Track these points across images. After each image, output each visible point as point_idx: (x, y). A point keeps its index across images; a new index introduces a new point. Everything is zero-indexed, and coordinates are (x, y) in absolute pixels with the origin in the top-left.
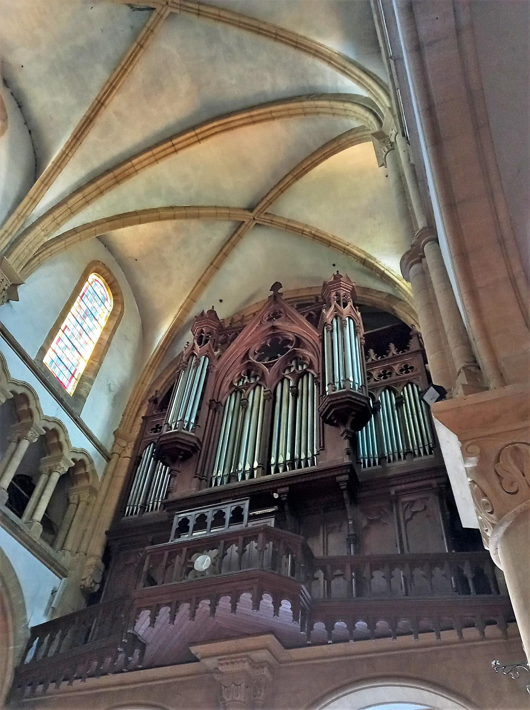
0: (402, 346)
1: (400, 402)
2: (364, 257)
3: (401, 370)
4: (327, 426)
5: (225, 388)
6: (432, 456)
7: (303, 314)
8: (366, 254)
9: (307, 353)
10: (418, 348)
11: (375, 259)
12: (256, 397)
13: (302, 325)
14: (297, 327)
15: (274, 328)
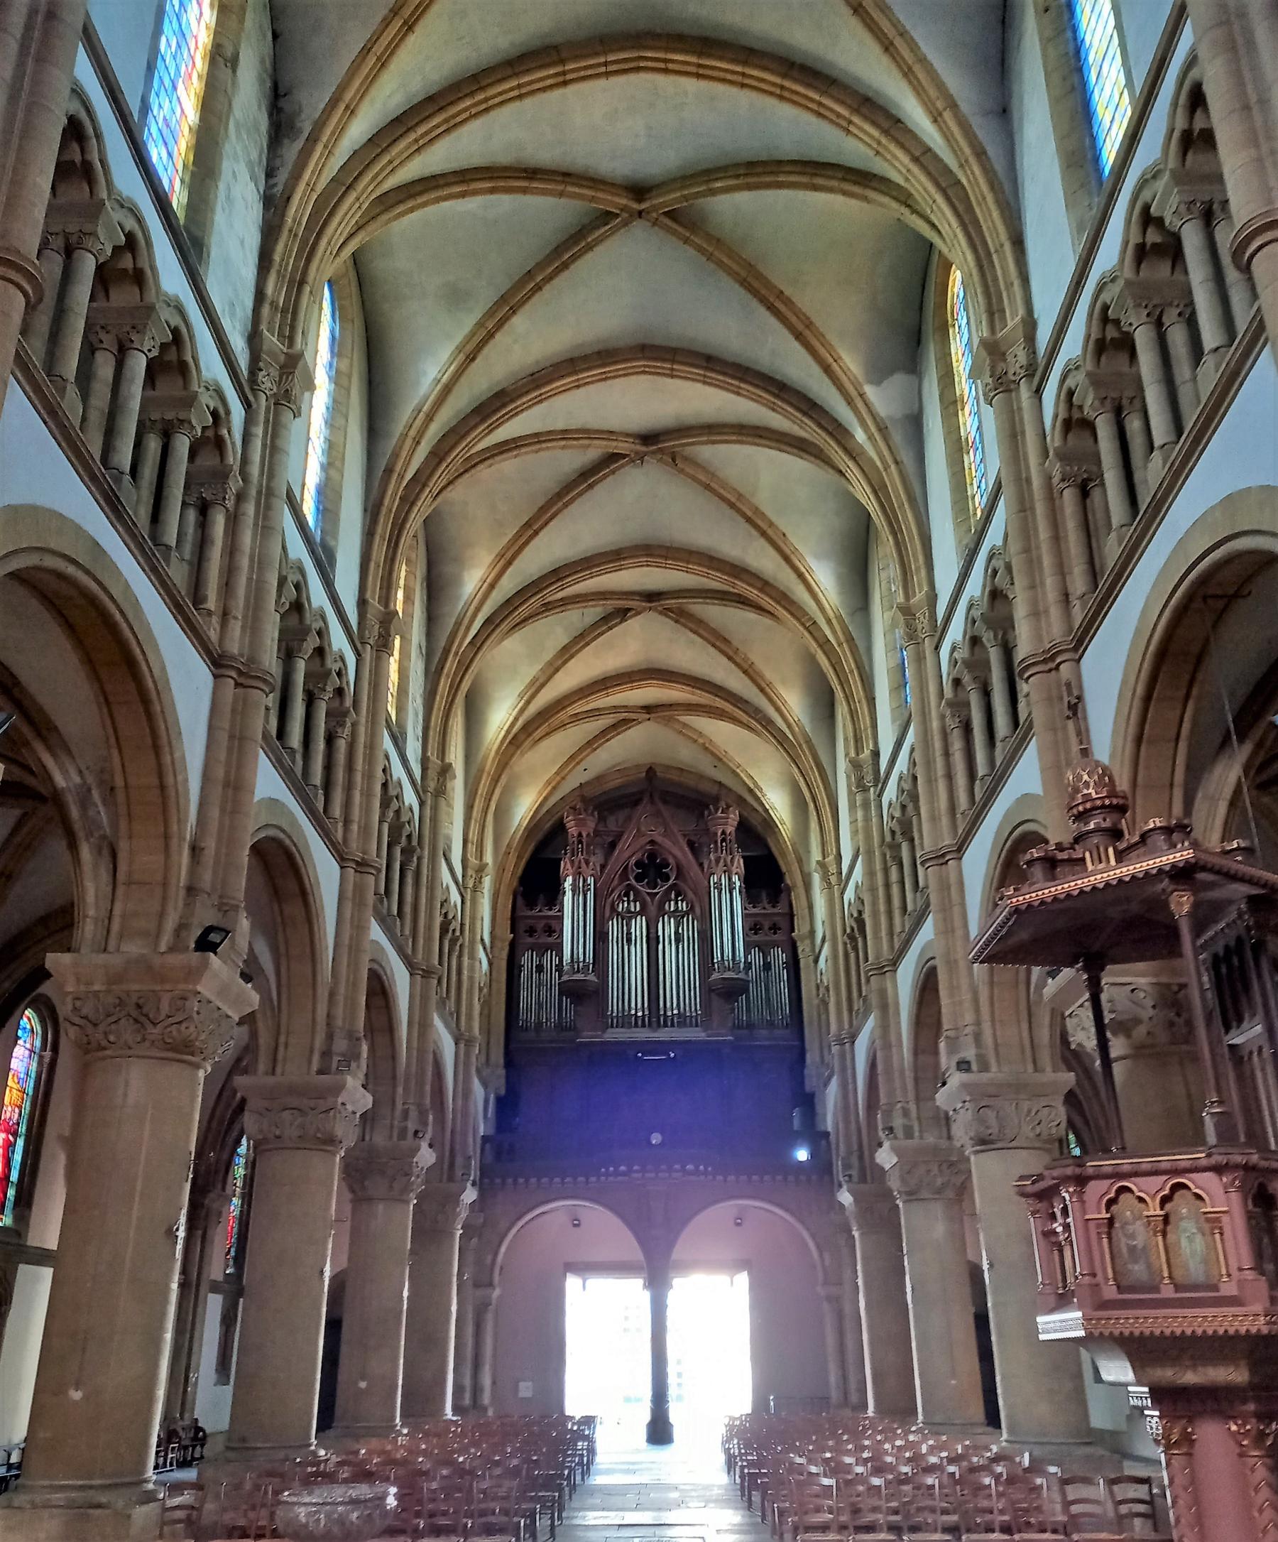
0: (774, 901)
1: (767, 967)
2: (752, 786)
3: (770, 929)
4: (713, 995)
5: (607, 914)
6: (788, 1031)
7: (685, 836)
8: (755, 783)
9: (686, 888)
10: (786, 910)
11: (761, 790)
12: (639, 927)
13: (681, 849)
14: (677, 851)
15: (652, 842)
